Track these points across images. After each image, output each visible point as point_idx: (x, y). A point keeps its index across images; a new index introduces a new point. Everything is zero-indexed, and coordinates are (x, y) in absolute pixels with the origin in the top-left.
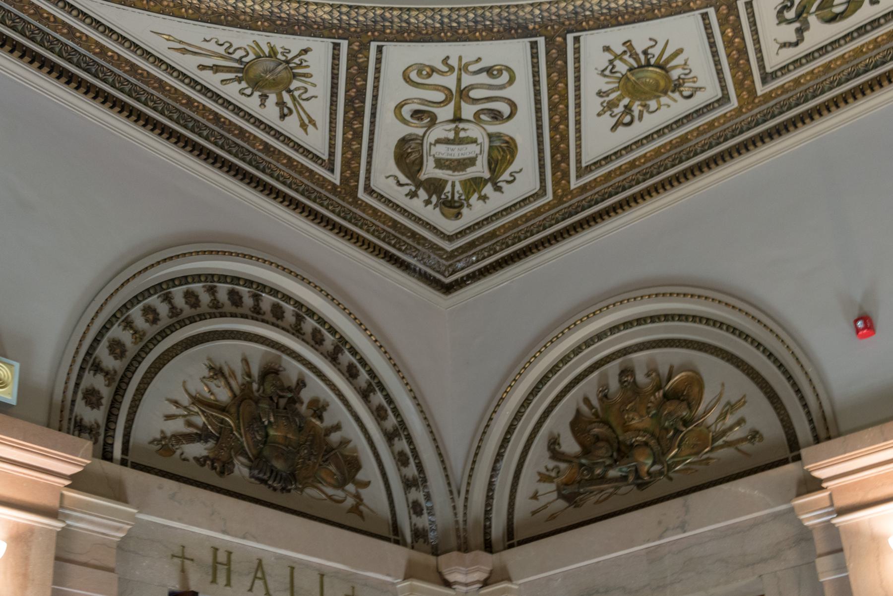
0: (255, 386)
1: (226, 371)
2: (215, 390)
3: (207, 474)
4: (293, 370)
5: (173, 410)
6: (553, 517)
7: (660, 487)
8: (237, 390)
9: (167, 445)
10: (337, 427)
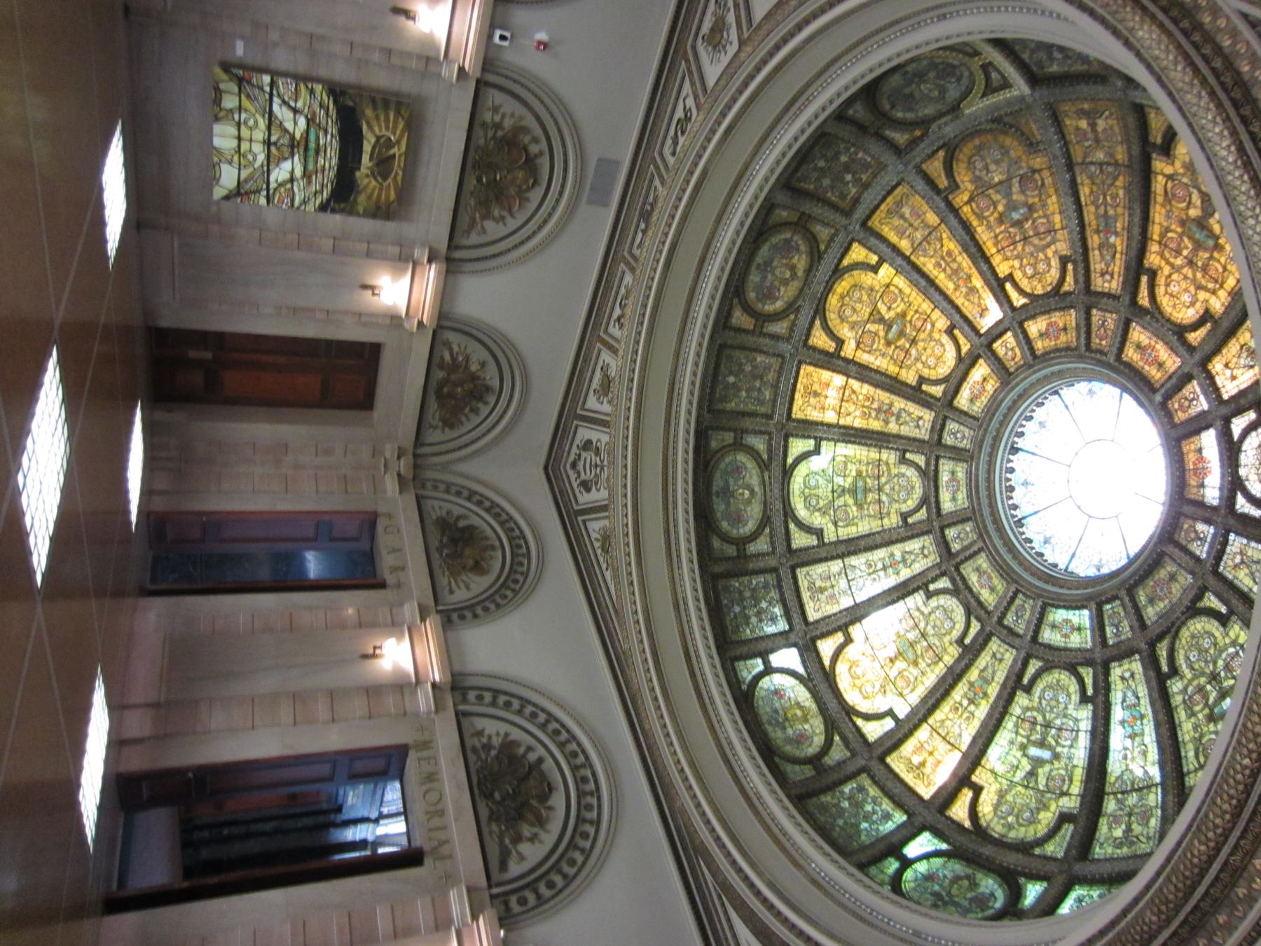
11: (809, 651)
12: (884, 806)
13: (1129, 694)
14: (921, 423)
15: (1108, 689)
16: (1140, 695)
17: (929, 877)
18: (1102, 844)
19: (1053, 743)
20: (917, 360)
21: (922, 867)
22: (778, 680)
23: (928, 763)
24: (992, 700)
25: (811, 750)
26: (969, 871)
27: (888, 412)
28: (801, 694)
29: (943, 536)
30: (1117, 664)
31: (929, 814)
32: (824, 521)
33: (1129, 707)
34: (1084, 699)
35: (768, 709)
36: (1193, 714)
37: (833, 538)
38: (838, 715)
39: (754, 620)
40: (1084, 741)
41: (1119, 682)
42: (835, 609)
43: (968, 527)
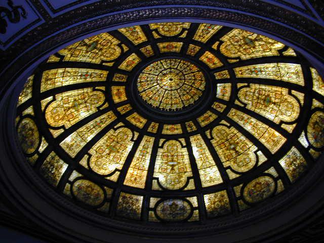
11: (80, 169)
12: (134, 198)
14: (102, 76)
17: (163, 210)
20: (101, 55)
21: (159, 208)
22: (76, 184)
23: (136, 177)
24: (150, 153)
25: (102, 197)
27: (87, 75)
28: (86, 183)
29: (117, 111)
31: (147, 191)
32: (63, 122)
35: (82, 196)
36: (221, 149)
37: (69, 126)
38: (101, 180)
39: (56, 173)
42: (80, 149)
43: (127, 106)
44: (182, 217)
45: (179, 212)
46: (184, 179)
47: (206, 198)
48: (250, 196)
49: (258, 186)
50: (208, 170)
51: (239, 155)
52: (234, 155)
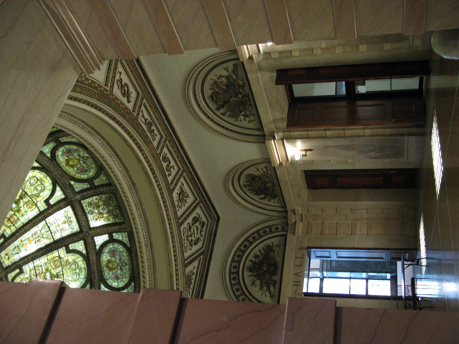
0: (254, 274)
1: (252, 281)
2: (257, 284)
3: (277, 286)
4: (248, 263)
5: (264, 295)
6: (280, 200)
7: (276, 182)
8: (256, 279)
9: (272, 296)
10: (260, 251)
13: (14, 252)
15: (15, 263)
16: (14, 247)
17: (117, 278)
18: (72, 229)
19: (43, 275)
26: (105, 268)
30: (3, 264)
33: (19, 250)
34: (21, 272)
36: (18, 219)
40: (37, 262)
41: (10, 260)
44: (125, 254)
45: (118, 258)
46: (71, 257)
47: (94, 224)
48: (86, 171)
49: (71, 163)
50: (53, 228)
51: (26, 193)
52: (26, 200)
